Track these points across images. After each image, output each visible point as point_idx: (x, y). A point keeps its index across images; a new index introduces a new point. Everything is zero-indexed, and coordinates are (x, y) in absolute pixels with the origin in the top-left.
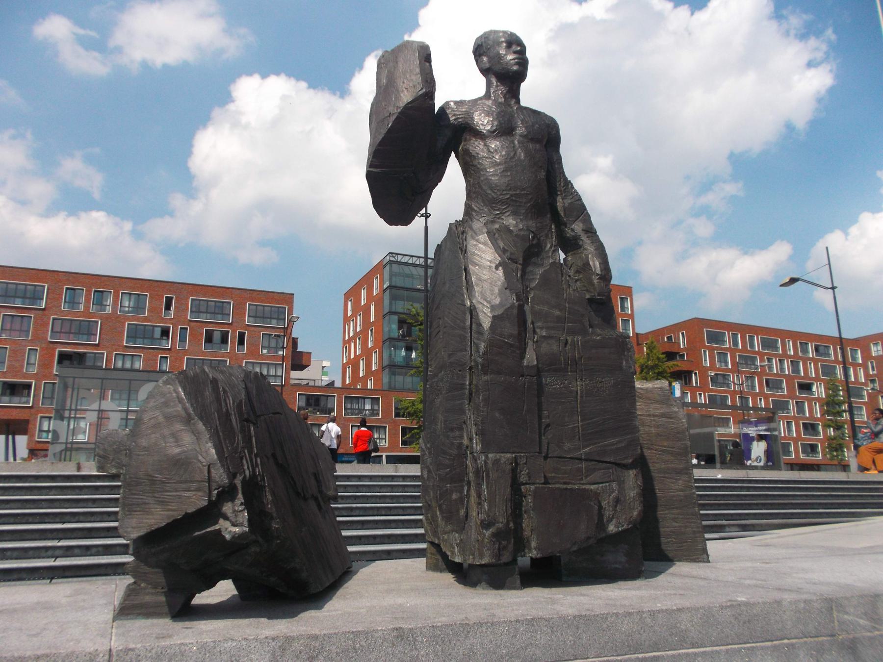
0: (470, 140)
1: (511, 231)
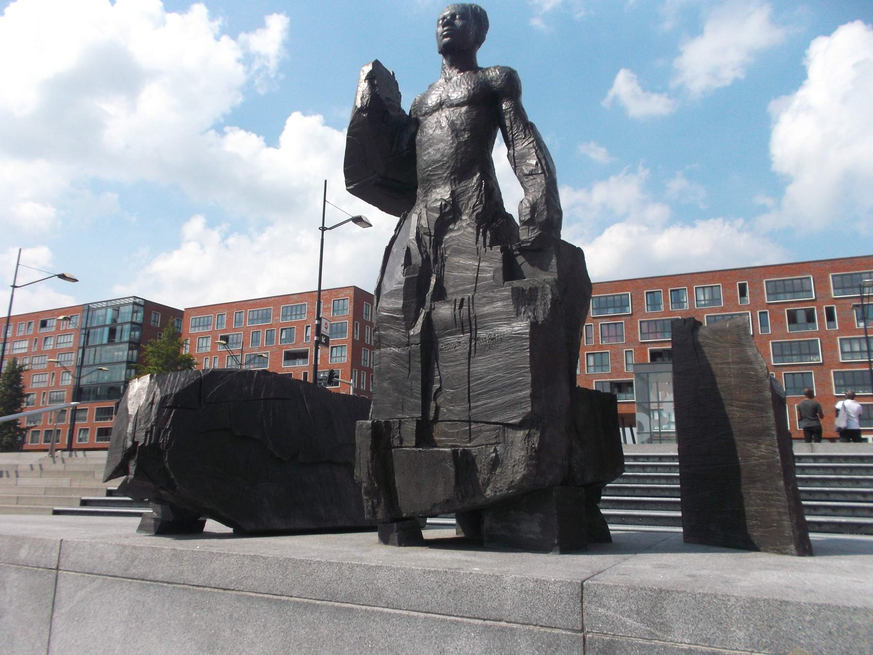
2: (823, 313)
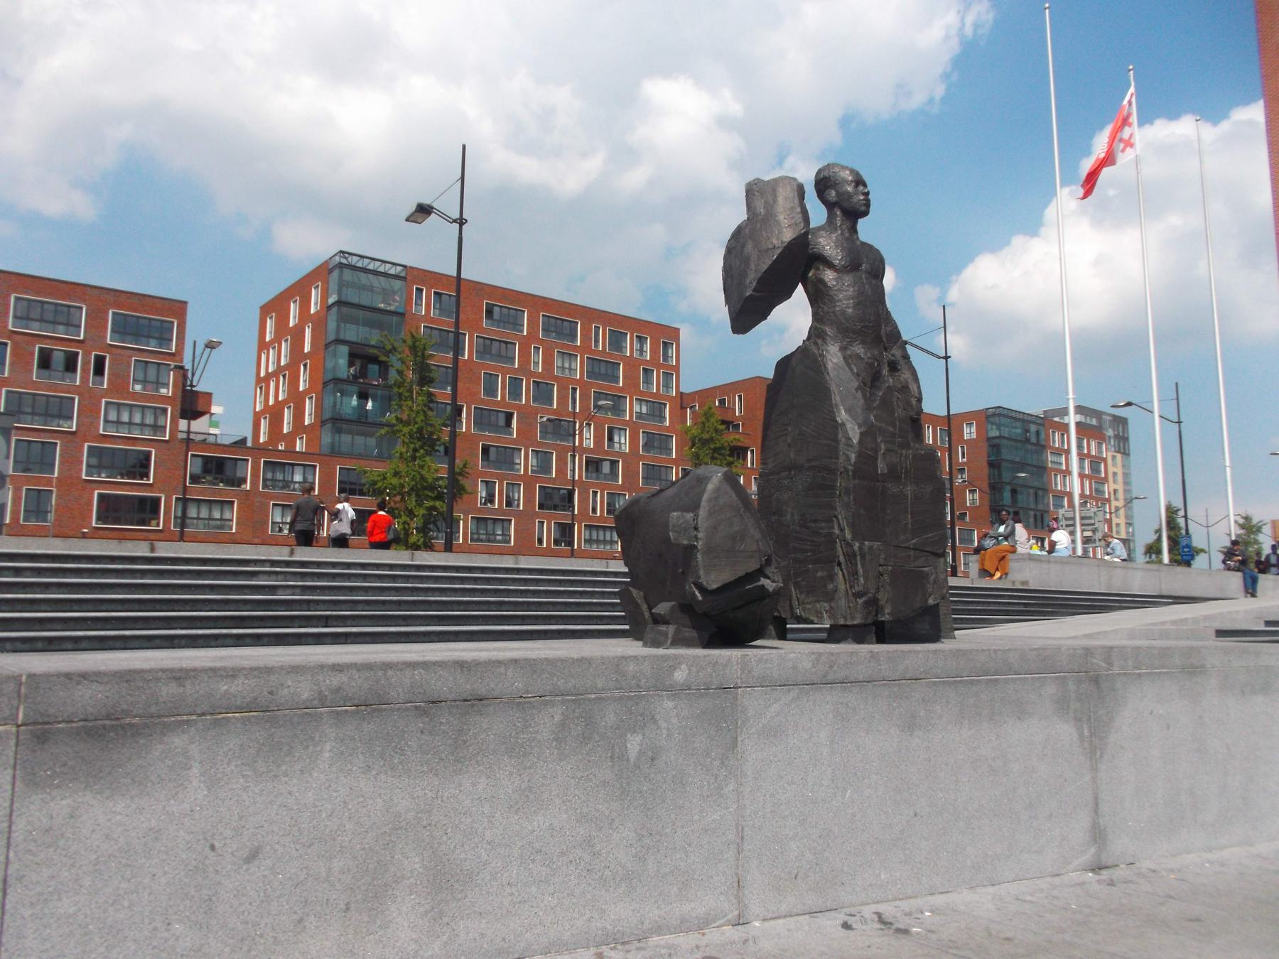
1: (862, 359)
2: (90, 362)
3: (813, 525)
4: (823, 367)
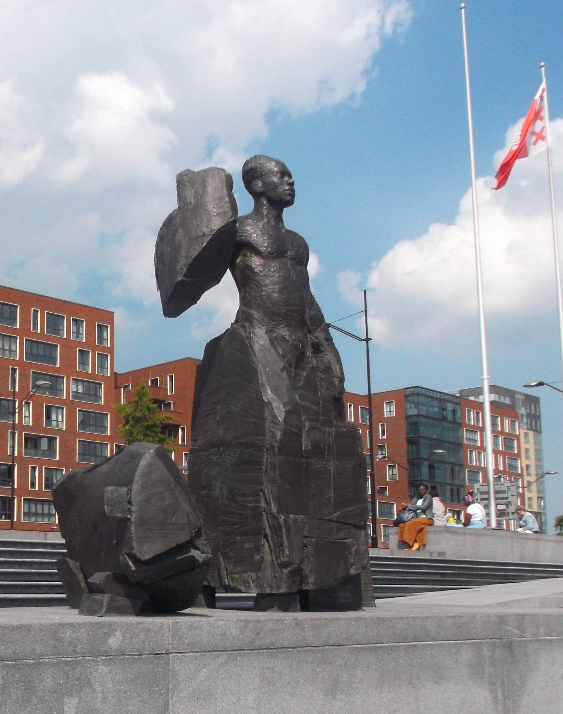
0: (252, 257)
1: (287, 341)
3: (241, 499)
4: (250, 350)
